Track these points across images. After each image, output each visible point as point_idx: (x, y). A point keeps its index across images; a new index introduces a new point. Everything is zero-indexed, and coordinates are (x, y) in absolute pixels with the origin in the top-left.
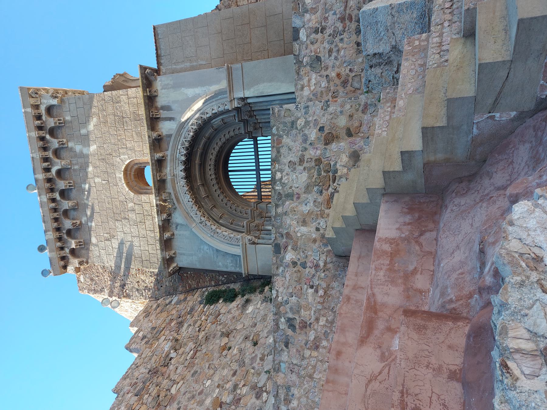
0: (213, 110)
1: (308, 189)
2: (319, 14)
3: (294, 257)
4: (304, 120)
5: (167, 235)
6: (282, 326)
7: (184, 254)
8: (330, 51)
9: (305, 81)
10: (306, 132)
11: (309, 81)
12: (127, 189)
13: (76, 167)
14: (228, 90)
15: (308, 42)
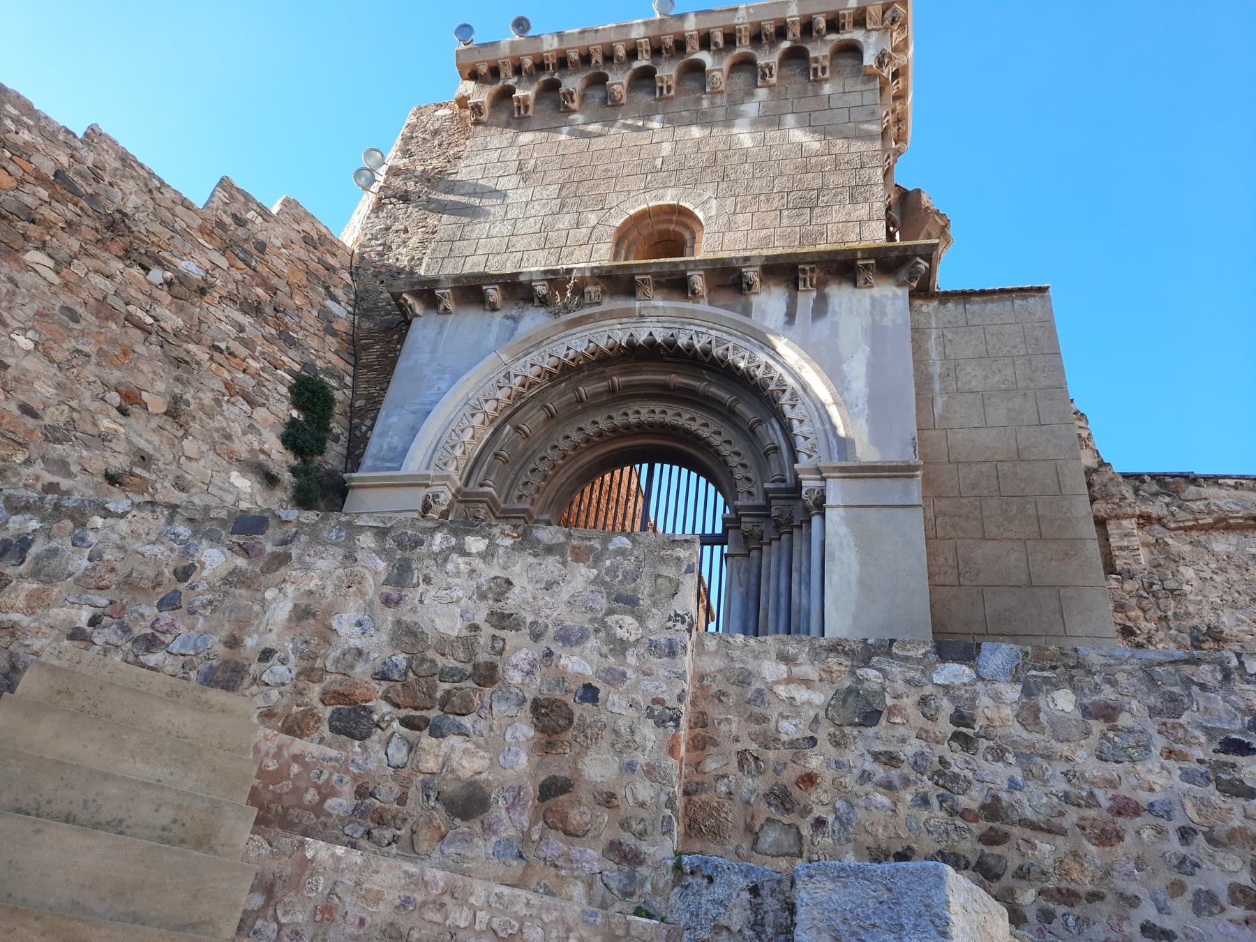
0: (801, 421)
1: (408, 634)
2: (1017, 730)
3: (205, 573)
4: (632, 639)
5: (494, 293)
7: (440, 333)
8: (891, 759)
9: (807, 669)
10: (592, 642)
11: (806, 682)
12: (632, 212)
13: (705, 104)
14: (849, 464)
15: (928, 690)
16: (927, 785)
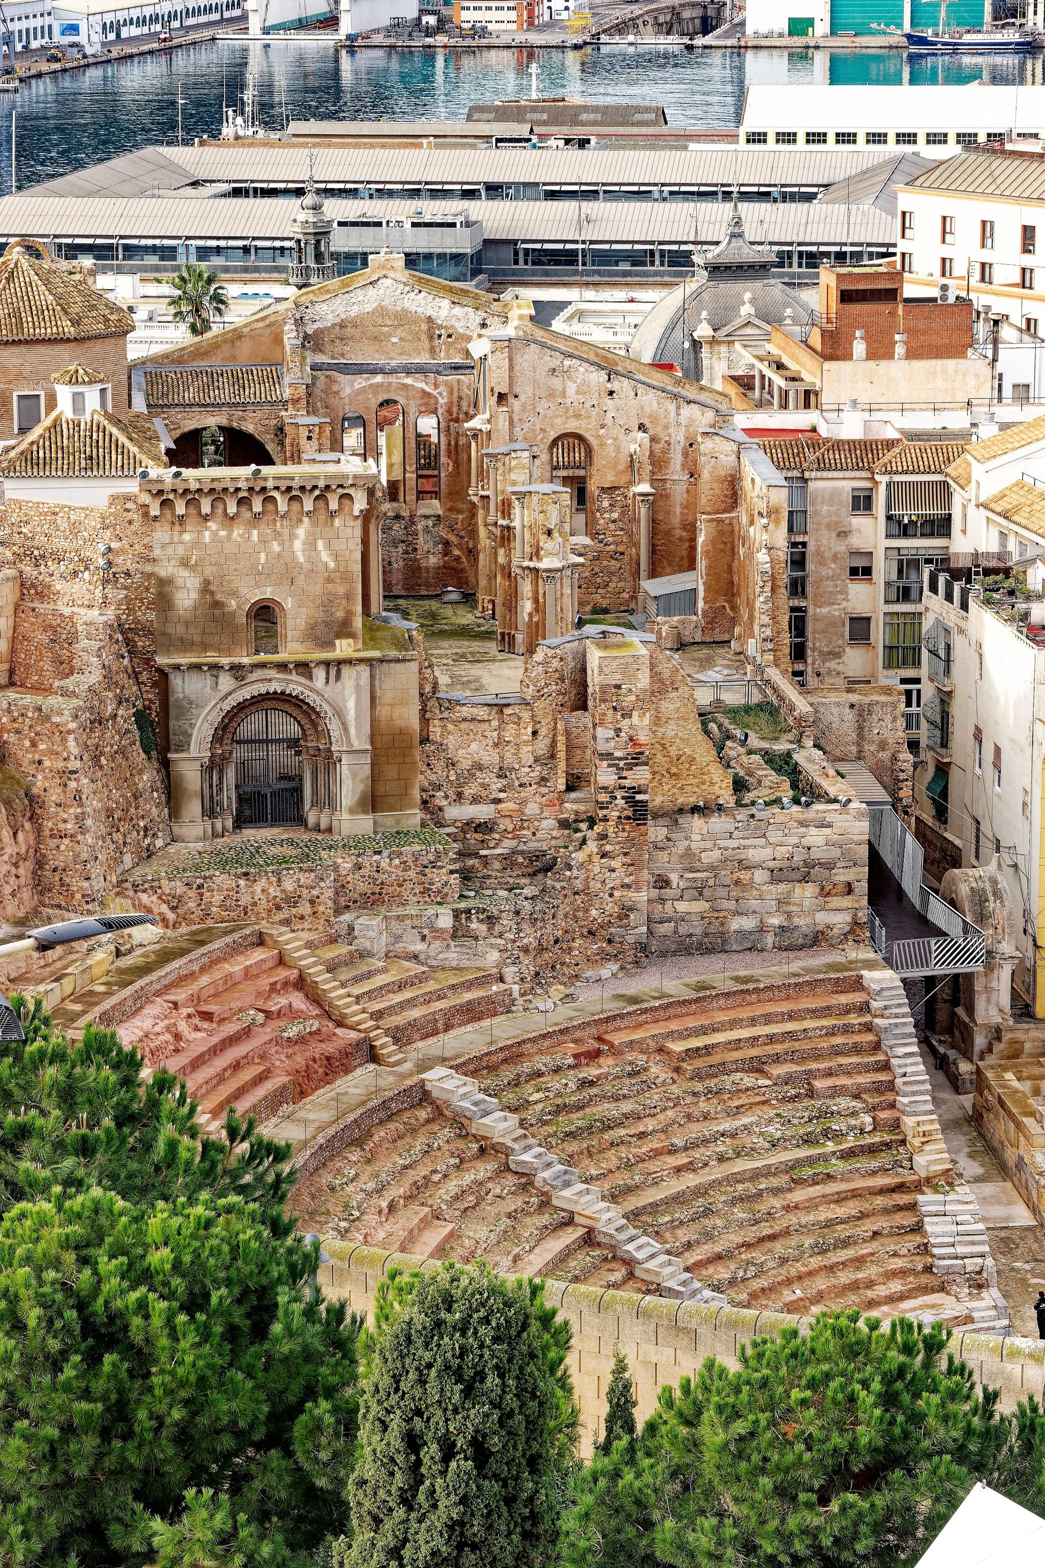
1: (283, 891)
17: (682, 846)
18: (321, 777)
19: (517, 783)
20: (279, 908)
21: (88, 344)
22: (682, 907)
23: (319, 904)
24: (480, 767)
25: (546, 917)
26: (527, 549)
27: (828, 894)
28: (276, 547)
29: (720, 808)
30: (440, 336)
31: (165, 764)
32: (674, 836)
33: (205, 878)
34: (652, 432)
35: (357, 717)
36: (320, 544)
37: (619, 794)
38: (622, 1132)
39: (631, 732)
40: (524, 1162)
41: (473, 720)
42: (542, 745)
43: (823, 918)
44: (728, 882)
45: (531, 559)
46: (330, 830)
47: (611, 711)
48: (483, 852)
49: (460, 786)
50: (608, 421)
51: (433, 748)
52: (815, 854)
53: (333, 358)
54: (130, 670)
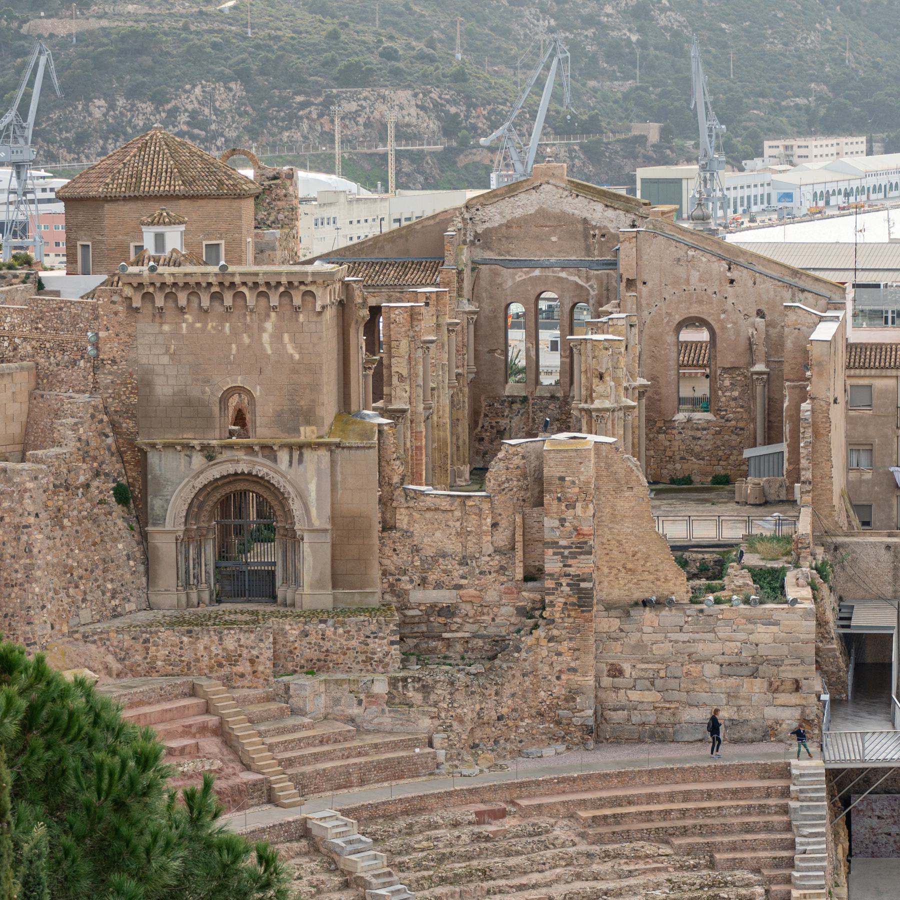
2: (333, 636)
6: (144, 635)
8: (310, 643)
9: (295, 627)
12: (225, 389)
16: (316, 647)
17: (634, 638)
18: (289, 554)
19: (477, 571)
20: (220, 665)
21: (201, 203)
22: (634, 696)
23: (259, 663)
24: (444, 556)
25: (487, 692)
26: (584, 392)
27: (776, 690)
28: (246, 339)
29: (670, 603)
30: (594, 236)
31: (144, 537)
32: (626, 627)
33: (151, 633)
34: (768, 318)
35: (319, 499)
36: (286, 337)
37: (564, 581)
38: (502, 882)
39: (576, 523)
40: (377, 895)
41: (437, 509)
42: (502, 538)
43: (771, 713)
44: (679, 674)
45: (586, 402)
46: (293, 605)
47: (556, 502)
48: (445, 635)
49: (424, 571)
50: (729, 307)
51: (398, 534)
52: (763, 651)
53: (500, 254)
54: (114, 449)
